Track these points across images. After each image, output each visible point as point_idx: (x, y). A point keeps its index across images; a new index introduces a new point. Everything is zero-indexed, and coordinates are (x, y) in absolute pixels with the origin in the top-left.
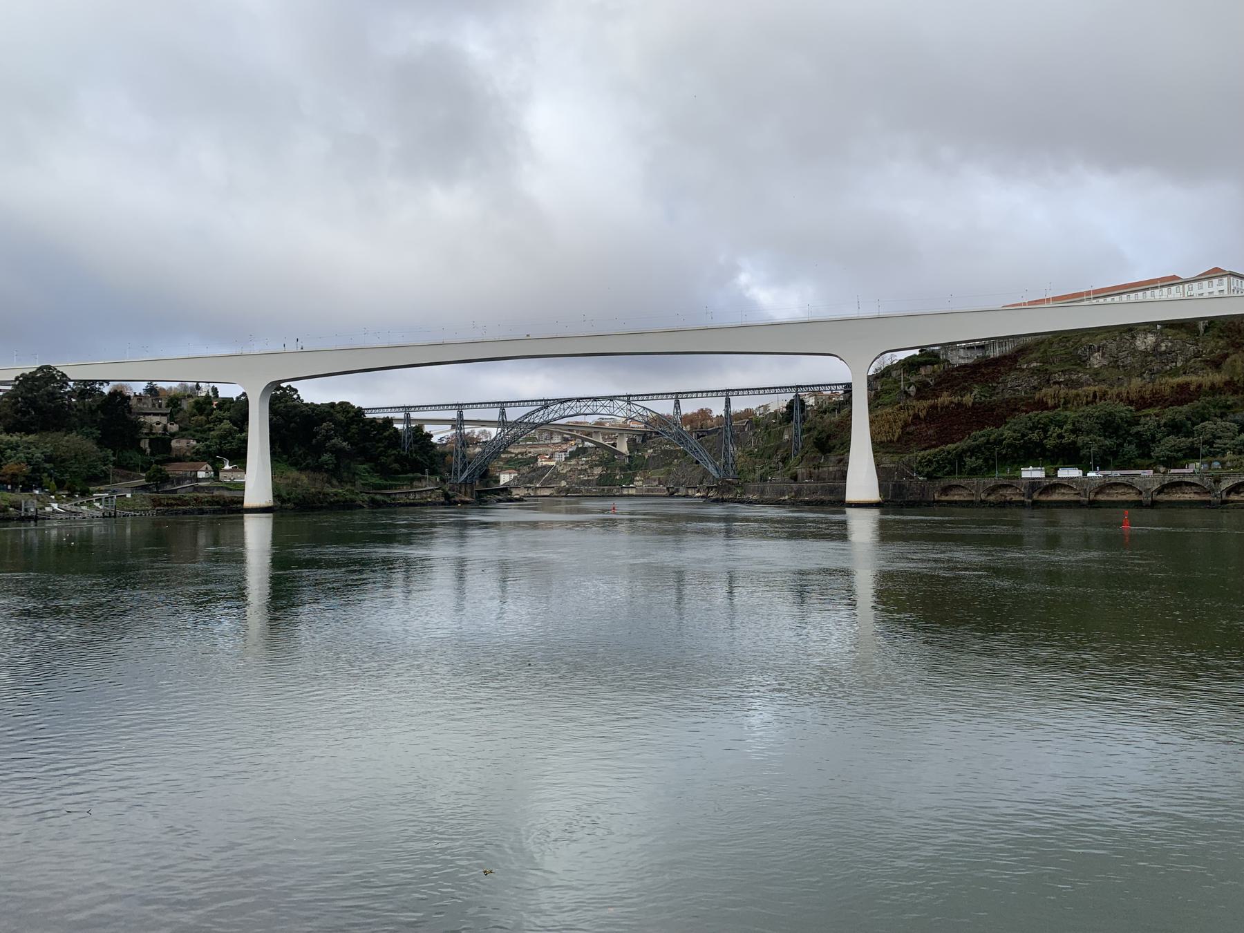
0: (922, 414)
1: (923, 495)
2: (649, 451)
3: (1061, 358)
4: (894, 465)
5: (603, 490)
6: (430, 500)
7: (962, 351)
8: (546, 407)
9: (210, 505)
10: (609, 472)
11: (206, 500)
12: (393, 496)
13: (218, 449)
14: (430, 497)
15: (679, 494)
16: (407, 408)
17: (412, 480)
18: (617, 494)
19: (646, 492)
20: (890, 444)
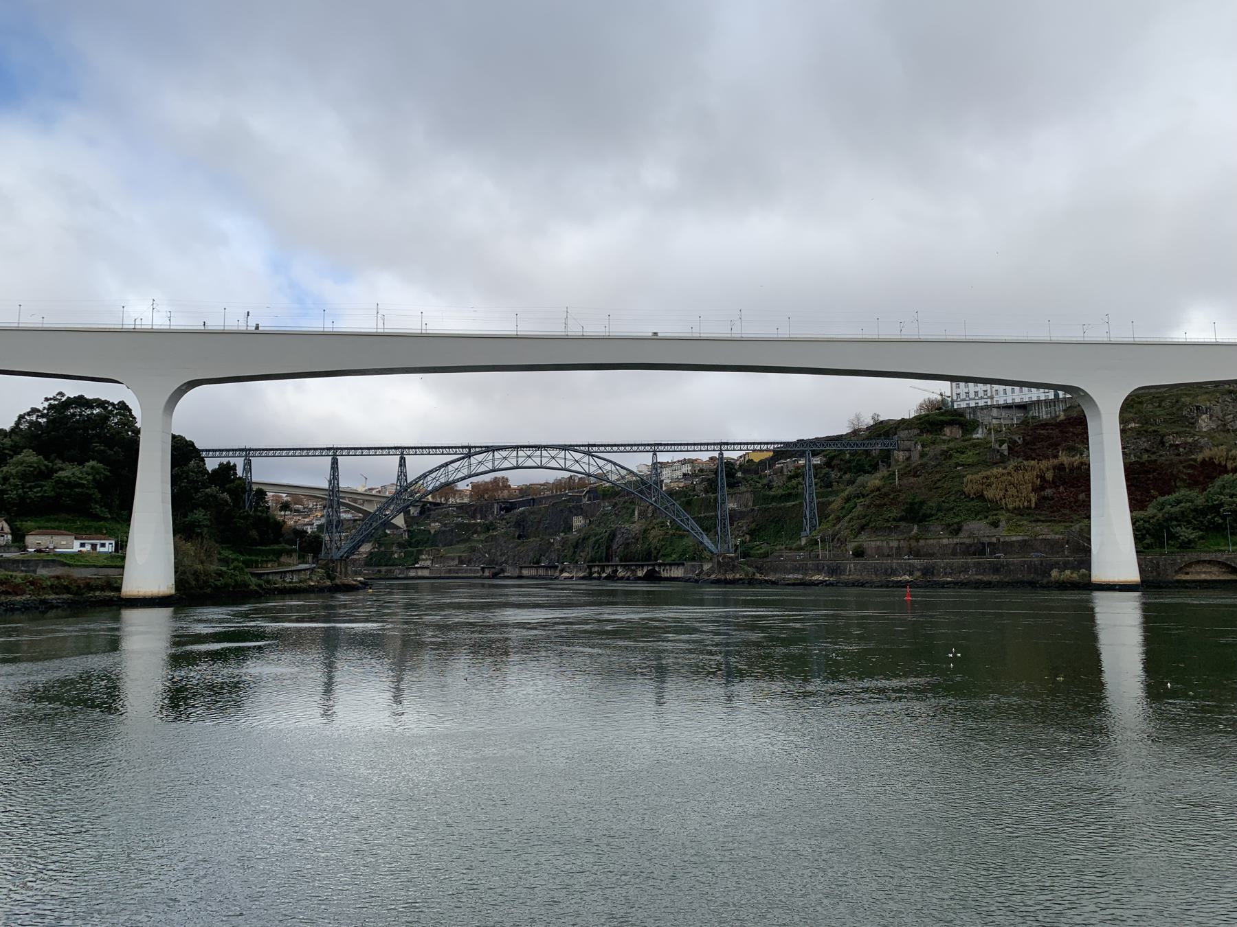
0: (1049, 476)
1: (1159, 574)
2: (433, 524)
3: (1164, 419)
4: (1061, 537)
5: (379, 571)
6: (312, 584)
7: (995, 410)
8: (469, 456)
9: (57, 594)
10: (382, 549)
11: (49, 583)
12: (265, 577)
13: (19, 496)
14: (310, 579)
15: (506, 574)
16: (248, 453)
17: (279, 554)
18: (400, 576)
19: (446, 573)
20: (1028, 511)
